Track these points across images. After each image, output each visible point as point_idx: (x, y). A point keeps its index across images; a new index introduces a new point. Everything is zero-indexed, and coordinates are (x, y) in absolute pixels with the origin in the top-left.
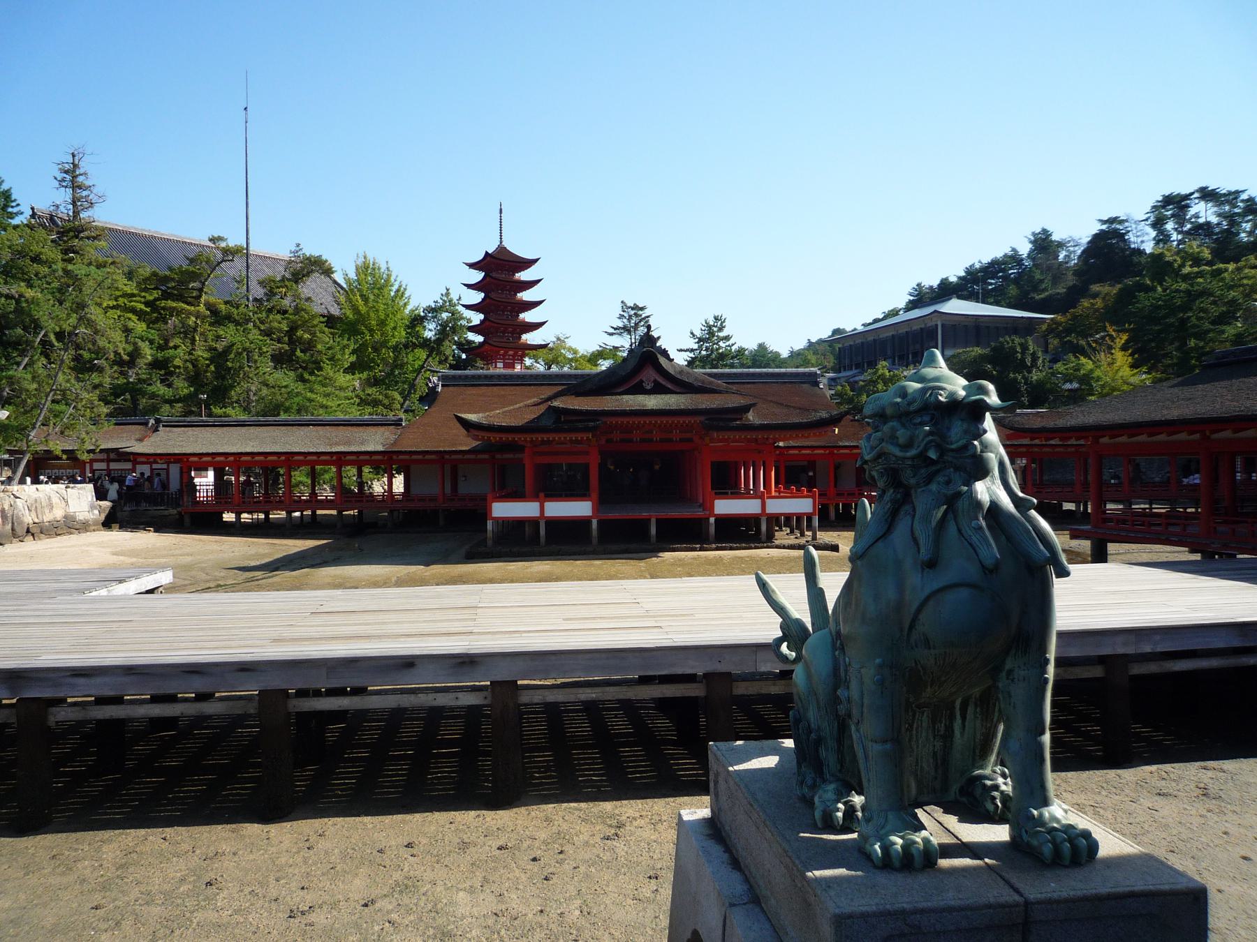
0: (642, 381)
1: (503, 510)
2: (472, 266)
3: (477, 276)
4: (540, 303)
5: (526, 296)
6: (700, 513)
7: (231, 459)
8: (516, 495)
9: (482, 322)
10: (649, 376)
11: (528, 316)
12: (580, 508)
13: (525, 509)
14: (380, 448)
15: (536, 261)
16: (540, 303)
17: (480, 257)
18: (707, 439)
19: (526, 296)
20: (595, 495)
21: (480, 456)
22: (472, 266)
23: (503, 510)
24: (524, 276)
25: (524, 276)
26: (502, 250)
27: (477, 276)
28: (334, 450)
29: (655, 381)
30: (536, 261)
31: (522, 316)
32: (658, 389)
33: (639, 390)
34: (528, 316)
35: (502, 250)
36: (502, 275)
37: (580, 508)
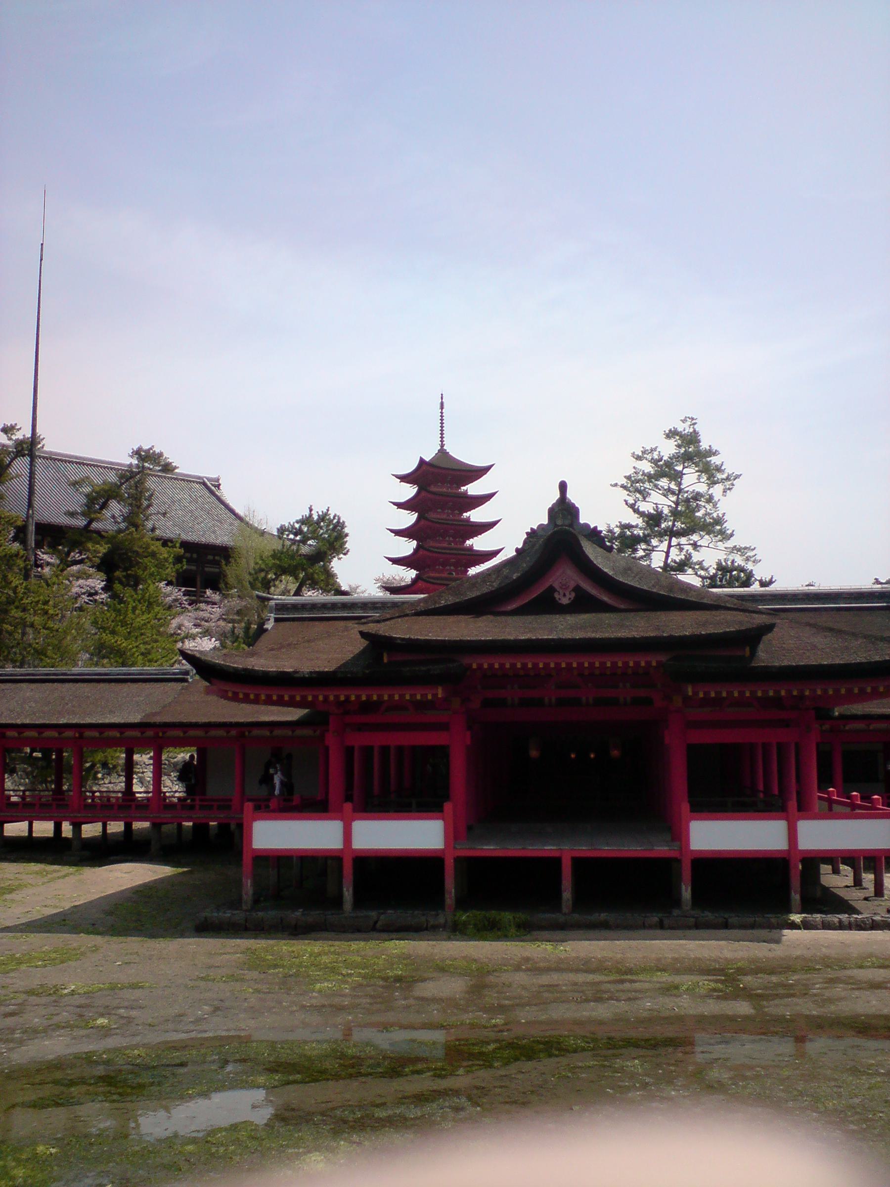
0: (551, 590)
1: (272, 835)
2: (404, 478)
3: (409, 491)
4: (494, 524)
5: (476, 515)
6: (661, 848)
7: (69, 734)
9: (416, 551)
10: (564, 580)
13: (315, 835)
14: (136, 718)
15: (488, 468)
16: (494, 524)
17: (410, 467)
18: (678, 701)
19: (476, 515)
21: (299, 732)
22: (404, 478)
23: (272, 835)
24: (473, 489)
25: (473, 489)
26: (442, 452)
27: (409, 491)
28: (63, 721)
29: (577, 589)
30: (488, 468)
31: (468, 543)
32: (583, 603)
33: (546, 605)
35: (442, 452)
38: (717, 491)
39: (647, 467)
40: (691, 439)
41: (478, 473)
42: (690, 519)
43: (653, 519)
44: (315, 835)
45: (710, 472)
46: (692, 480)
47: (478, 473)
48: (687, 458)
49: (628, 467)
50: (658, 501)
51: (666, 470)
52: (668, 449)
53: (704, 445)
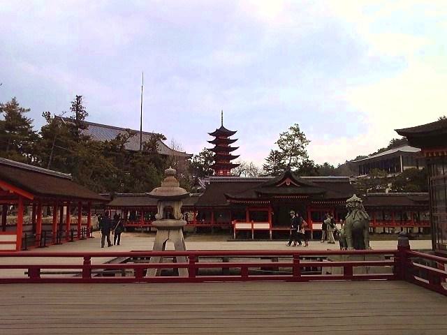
3: (213, 138)
5: (232, 145)
8: (243, 220)
11: (233, 153)
12: (266, 226)
13: (247, 226)
14: (193, 205)
19: (232, 145)
20: (270, 221)
24: (231, 138)
25: (231, 138)
27: (213, 138)
34: (233, 153)
36: (222, 138)
37: (266, 226)
38: (304, 145)
39: (286, 138)
40: (298, 130)
41: (234, 133)
42: (295, 151)
43: (287, 151)
44: (247, 226)
45: (302, 139)
46: (297, 141)
47: (234, 133)
48: (296, 135)
49: (278, 138)
50: (287, 146)
51: (290, 138)
52: (291, 132)
53: (301, 132)
